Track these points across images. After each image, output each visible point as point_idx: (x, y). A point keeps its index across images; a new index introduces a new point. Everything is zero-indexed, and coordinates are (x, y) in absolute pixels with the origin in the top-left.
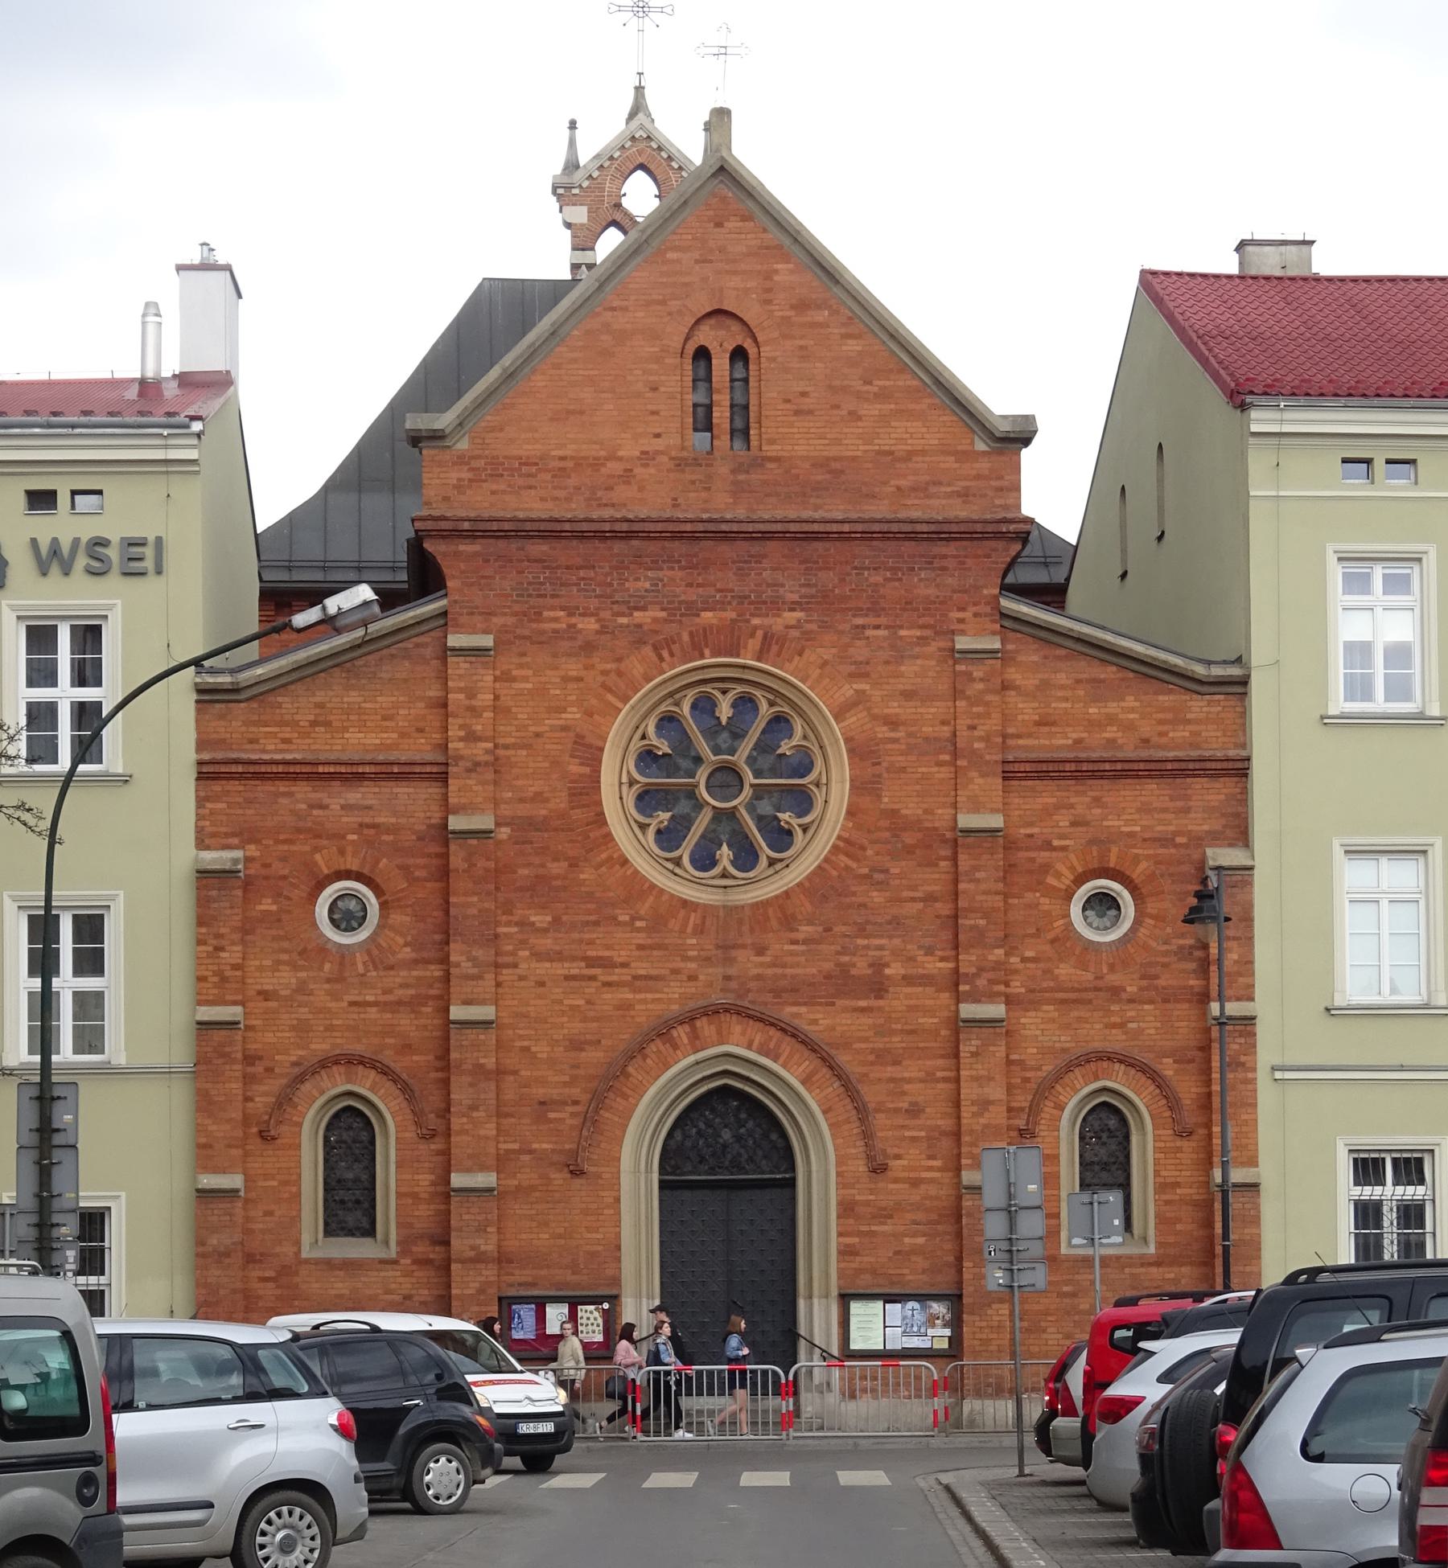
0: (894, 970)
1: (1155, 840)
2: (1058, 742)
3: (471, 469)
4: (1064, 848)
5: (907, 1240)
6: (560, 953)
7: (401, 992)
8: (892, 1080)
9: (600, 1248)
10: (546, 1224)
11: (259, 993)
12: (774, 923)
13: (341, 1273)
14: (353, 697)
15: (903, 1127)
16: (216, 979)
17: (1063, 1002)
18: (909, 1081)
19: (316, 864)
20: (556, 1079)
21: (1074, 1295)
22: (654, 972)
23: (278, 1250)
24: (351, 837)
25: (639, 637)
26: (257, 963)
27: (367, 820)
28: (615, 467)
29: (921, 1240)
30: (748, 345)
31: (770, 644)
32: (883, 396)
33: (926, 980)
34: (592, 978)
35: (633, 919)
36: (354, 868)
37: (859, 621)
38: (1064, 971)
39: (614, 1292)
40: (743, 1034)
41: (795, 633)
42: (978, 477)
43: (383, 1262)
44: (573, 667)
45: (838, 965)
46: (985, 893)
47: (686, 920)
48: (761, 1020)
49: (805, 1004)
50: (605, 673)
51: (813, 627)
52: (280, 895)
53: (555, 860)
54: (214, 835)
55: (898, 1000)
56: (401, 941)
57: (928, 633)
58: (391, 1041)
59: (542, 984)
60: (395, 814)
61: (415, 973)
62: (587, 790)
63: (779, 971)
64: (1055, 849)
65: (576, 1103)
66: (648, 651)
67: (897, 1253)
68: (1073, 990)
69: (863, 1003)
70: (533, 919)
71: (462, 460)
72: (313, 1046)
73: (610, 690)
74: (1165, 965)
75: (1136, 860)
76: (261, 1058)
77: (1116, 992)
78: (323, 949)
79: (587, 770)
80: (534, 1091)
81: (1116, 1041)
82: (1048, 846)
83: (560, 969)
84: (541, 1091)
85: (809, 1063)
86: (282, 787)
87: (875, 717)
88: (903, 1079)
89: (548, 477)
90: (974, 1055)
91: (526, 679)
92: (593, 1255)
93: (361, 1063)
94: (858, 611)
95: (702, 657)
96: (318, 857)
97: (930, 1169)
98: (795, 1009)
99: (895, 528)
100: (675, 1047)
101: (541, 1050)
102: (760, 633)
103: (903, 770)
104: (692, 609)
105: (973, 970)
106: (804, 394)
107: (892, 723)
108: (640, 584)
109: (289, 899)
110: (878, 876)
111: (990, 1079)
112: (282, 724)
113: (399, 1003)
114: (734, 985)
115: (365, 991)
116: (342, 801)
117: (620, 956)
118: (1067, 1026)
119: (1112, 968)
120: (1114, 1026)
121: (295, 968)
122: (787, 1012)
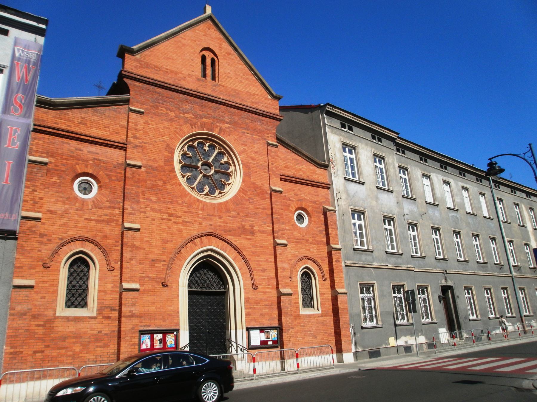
0: (256, 228)
1: (312, 202)
2: (290, 173)
3: (140, 64)
4: (293, 201)
5: (264, 310)
6: (160, 210)
7: (104, 217)
8: (258, 261)
9: (172, 313)
11: (48, 211)
12: (224, 211)
14: (95, 118)
15: (261, 275)
16: (32, 202)
17: (296, 242)
18: (262, 261)
19: (76, 169)
20: (158, 252)
21: (304, 326)
22: (189, 220)
24: (90, 162)
25: (186, 121)
27: (96, 157)
28: (180, 75)
29: (267, 310)
30: (215, 58)
32: (247, 79)
34: (170, 220)
35: (183, 203)
36: (91, 172)
38: (295, 233)
39: (177, 328)
40: (216, 243)
41: (228, 130)
42: (270, 104)
43: (91, 318)
44: (167, 124)
45: (241, 225)
47: (198, 206)
48: (221, 239)
49: (233, 236)
50: (176, 128)
51: (233, 129)
52: (61, 176)
53: (159, 180)
55: (258, 237)
56: (106, 199)
57: (260, 138)
58: (100, 234)
59: (154, 220)
60: (106, 157)
61: (110, 211)
62: (169, 161)
65: (164, 261)
66: (189, 125)
67: (261, 314)
69: (248, 237)
70: (151, 198)
71: (137, 60)
72: (68, 233)
73: (177, 133)
74: (317, 235)
75: (309, 206)
77: (307, 240)
78: (76, 198)
79: (170, 155)
80: (150, 256)
82: (289, 199)
83: (160, 216)
84: (153, 256)
85: (235, 253)
86: (66, 140)
87: (248, 157)
89: (162, 72)
90: (280, 254)
91: (153, 125)
93: (88, 241)
94: (243, 128)
96: (77, 166)
97: (269, 288)
98: (230, 237)
99: (253, 110)
100: (196, 245)
101: (153, 242)
102: (219, 128)
103: (256, 172)
104: (201, 117)
106: (229, 73)
107: (253, 159)
108: (187, 107)
109: (64, 179)
110: (252, 201)
112: (68, 120)
113: (103, 221)
114: (212, 227)
115: (91, 215)
116: (88, 150)
117: (179, 214)
119: (306, 233)
121: (64, 203)
122: (228, 237)
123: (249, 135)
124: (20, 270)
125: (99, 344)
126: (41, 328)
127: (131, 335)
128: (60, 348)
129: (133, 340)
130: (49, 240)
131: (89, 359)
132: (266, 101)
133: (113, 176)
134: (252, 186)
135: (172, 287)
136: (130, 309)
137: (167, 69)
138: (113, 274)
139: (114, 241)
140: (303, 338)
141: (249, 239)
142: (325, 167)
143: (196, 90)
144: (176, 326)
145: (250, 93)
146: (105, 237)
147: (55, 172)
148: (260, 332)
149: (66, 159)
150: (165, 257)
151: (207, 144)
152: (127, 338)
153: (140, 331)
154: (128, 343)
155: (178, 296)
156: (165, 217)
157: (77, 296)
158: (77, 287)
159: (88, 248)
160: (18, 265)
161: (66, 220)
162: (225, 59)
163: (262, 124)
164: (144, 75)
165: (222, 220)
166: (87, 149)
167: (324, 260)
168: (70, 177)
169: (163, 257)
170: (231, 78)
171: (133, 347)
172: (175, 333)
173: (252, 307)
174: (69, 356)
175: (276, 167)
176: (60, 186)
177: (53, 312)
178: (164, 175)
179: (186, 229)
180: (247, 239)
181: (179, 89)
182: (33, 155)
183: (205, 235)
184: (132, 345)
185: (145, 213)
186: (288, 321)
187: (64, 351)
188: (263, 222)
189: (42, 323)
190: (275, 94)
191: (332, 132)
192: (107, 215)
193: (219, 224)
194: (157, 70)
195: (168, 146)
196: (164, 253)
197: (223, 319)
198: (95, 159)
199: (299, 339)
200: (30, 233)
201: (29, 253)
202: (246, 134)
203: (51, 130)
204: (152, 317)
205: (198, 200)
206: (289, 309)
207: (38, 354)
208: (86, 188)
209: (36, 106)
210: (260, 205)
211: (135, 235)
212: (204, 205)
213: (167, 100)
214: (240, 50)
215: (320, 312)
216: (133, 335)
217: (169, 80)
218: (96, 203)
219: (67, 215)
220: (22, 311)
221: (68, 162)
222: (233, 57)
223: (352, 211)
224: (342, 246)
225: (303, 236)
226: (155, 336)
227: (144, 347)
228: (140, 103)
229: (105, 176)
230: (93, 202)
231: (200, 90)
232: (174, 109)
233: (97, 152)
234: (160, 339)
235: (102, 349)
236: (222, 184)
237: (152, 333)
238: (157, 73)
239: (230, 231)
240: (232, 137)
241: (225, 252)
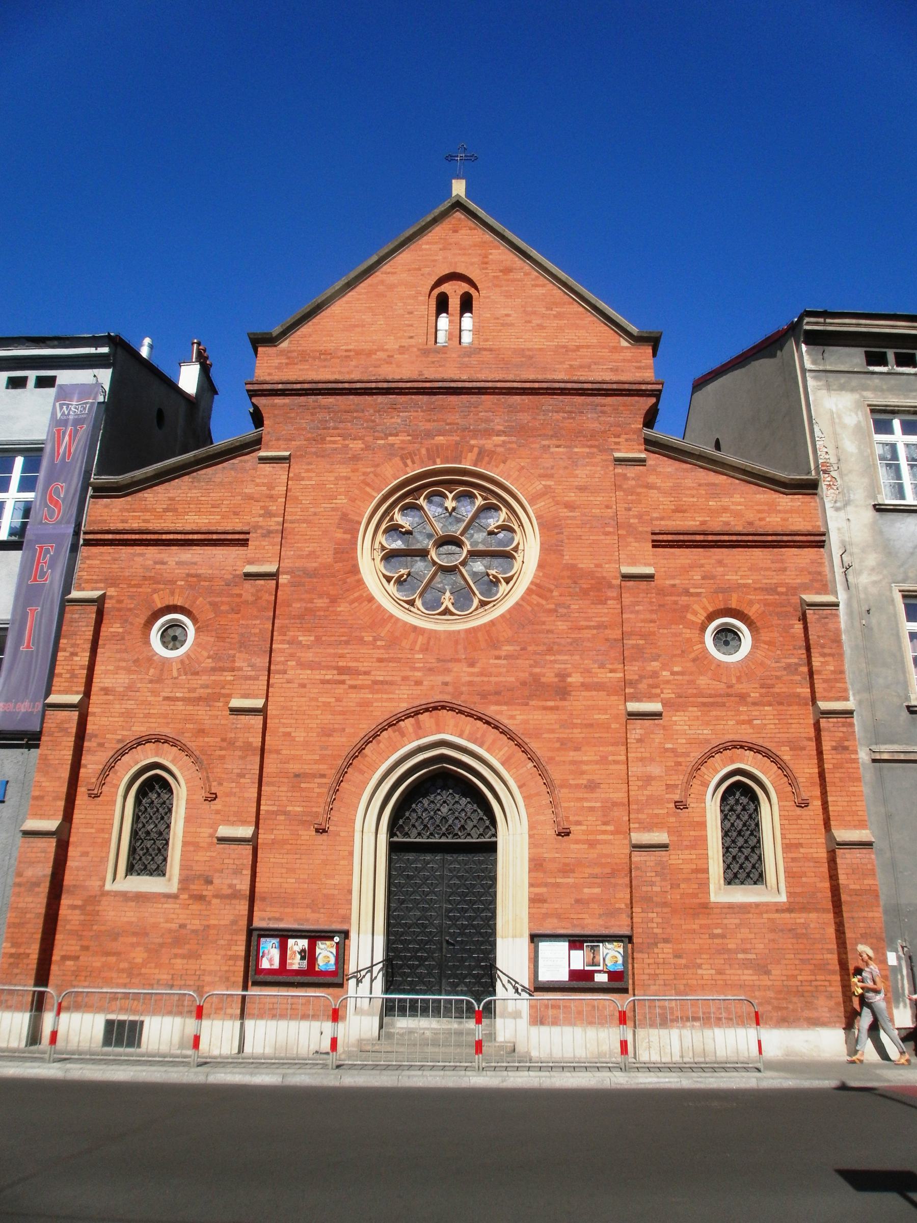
0: (575, 679)
1: (762, 589)
3: (288, 358)
4: (698, 594)
5: (586, 890)
6: (319, 663)
7: (202, 690)
8: (573, 763)
9: (336, 892)
10: (291, 870)
12: (483, 645)
13: (133, 904)
14: (195, 493)
15: (582, 799)
16: (68, 676)
17: (704, 704)
20: (310, 757)
21: (723, 936)
22: (388, 678)
24: (179, 583)
26: (103, 668)
27: (192, 572)
28: (381, 355)
29: (597, 890)
30: (472, 291)
31: (482, 455)
32: (558, 316)
33: (599, 687)
34: (343, 682)
35: (375, 639)
37: (544, 443)
38: (703, 681)
39: (345, 927)
40: (456, 726)
41: (500, 450)
42: (624, 360)
43: (168, 896)
44: (344, 471)
45: (531, 674)
46: (643, 621)
47: (415, 642)
48: (471, 716)
49: (506, 704)
50: (365, 474)
51: (514, 446)
52: (126, 621)
53: (321, 596)
54: (87, 581)
55: (579, 702)
56: (205, 654)
57: (595, 450)
58: (191, 726)
59: (303, 686)
60: (211, 567)
61: (213, 678)
63: (486, 679)
64: (692, 595)
65: (323, 776)
67: (578, 901)
68: (710, 696)
70: (300, 638)
71: (282, 353)
72: (134, 729)
73: (368, 485)
74: (777, 678)
75: (751, 603)
76: (96, 736)
77: (743, 698)
78: (151, 659)
79: (348, 536)
80: (292, 766)
81: (745, 734)
82: (687, 593)
83: (318, 675)
84: (297, 766)
85: (508, 747)
86: (138, 549)
88: (582, 762)
89: (338, 361)
90: (639, 741)
91: (310, 479)
92: (327, 896)
93: (166, 742)
94: (545, 436)
95: (435, 463)
96: (155, 596)
97: (604, 832)
99: (569, 386)
100: (403, 735)
101: (300, 735)
102: (476, 450)
103: (579, 537)
104: (429, 434)
105: (636, 677)
106: (507, 315)
107: (570, 506)
108: (393, 420)
109: (131, 624)
110: (562, 611)
111: (652, 760)
112: (145, 510)
113: (200, 699)
114: (450, 689)
115: (175, 690)
116: (177, 559)
117: (363, 666)
118: (707, 724)
119: (739, 679)
120: (743, 722)
121: (129, 671)
122: (492, 710)
123: (561, 450)
124: (41, 803)
125: (180, 951)
126: (77, 912)
127: (229, 937)
128: (108, 954)
130: (101, 745)
131: (159, 981)
132: (616, 356)
133: (222, 603)
134: (566, 573)
135: (337, 834)
136: (229, 881)
137: (349, 351)
138: (213, 807)
139: (218, 740)
140: (720, 972)
141: (551, 709)
142: (810, 487)
143: (415, 377)
144: (342, 922)
145: (564, 347)
146: (201, 732)
147: (117, 613)
148: (570, 948)
149: (135, 586)
150: (325, 767)
151: (450, 496)
152: (222, 942)
154: (222, 952)
155: (351, 854)
156: (328, 677)
157: (147, 854)
158: (153, 835)
159: (167, 757)
160: (37, 793)
161: (130, 705)
162: (496, 286)
163: (592, 415)
164: (293, 378)
165: (476, 670)
166: (176, 559)
167: (803, 748)
168: (141, 620)
169: (321, 767)
170: (512, 325)
171: (231, 963)
172: (337, 939)
173: (549, 880)
174: (123, 971)
175: (640, 516)
176: (123, 639)
177: (99, 883)
178: (333, 584)
179: (381, 700)
180: (545, 708)
181: (373, 385)
182: (83, 589)
183: (427, 710)
184: (232, 958)
185: (285, 672)
186: (652, 921)
187: (113, 959)
188: (595, 662)
189: (79, 903)
190: (634, 330)
191: (829, 388)
192: (207, 687)
193: (468, 679)
194: (325, 360)
195: (344, 517)
197: (489, 910)
198: (188, 575)
199: (706, 972)
200: (59, 734)
202: (553, 450)
203: (110, 537)
205: (415, 628)
206: (656, 889)
207: (69, 963)
208: (172, 637)
209: (92, 497)
210: (588, 619)
211: (252, 722)
213: (348, 416)
214: (534, 253)
215: (783, 898)
216: (235, 937)
217: (352, 372)
218: (187, 666)
219: (134, 693)
220: (34, 880)
221: (140, 590)
222: (520, 275)
223: (904, 597)
224: (860, 703)
225: (730, 687)
226: (291, 942)
227: (265, 964)
228: (286, 440)
229: (208, 606)
230: (182, 662)
231: (430, 374)
233: (195, 560)
234: (303, 951)
235: (185, 961)
236: (491, 581)
237: (283, 936)
238: (325, 367)
239: (497, 693)
240: (511, 464)
241: (481, 746)
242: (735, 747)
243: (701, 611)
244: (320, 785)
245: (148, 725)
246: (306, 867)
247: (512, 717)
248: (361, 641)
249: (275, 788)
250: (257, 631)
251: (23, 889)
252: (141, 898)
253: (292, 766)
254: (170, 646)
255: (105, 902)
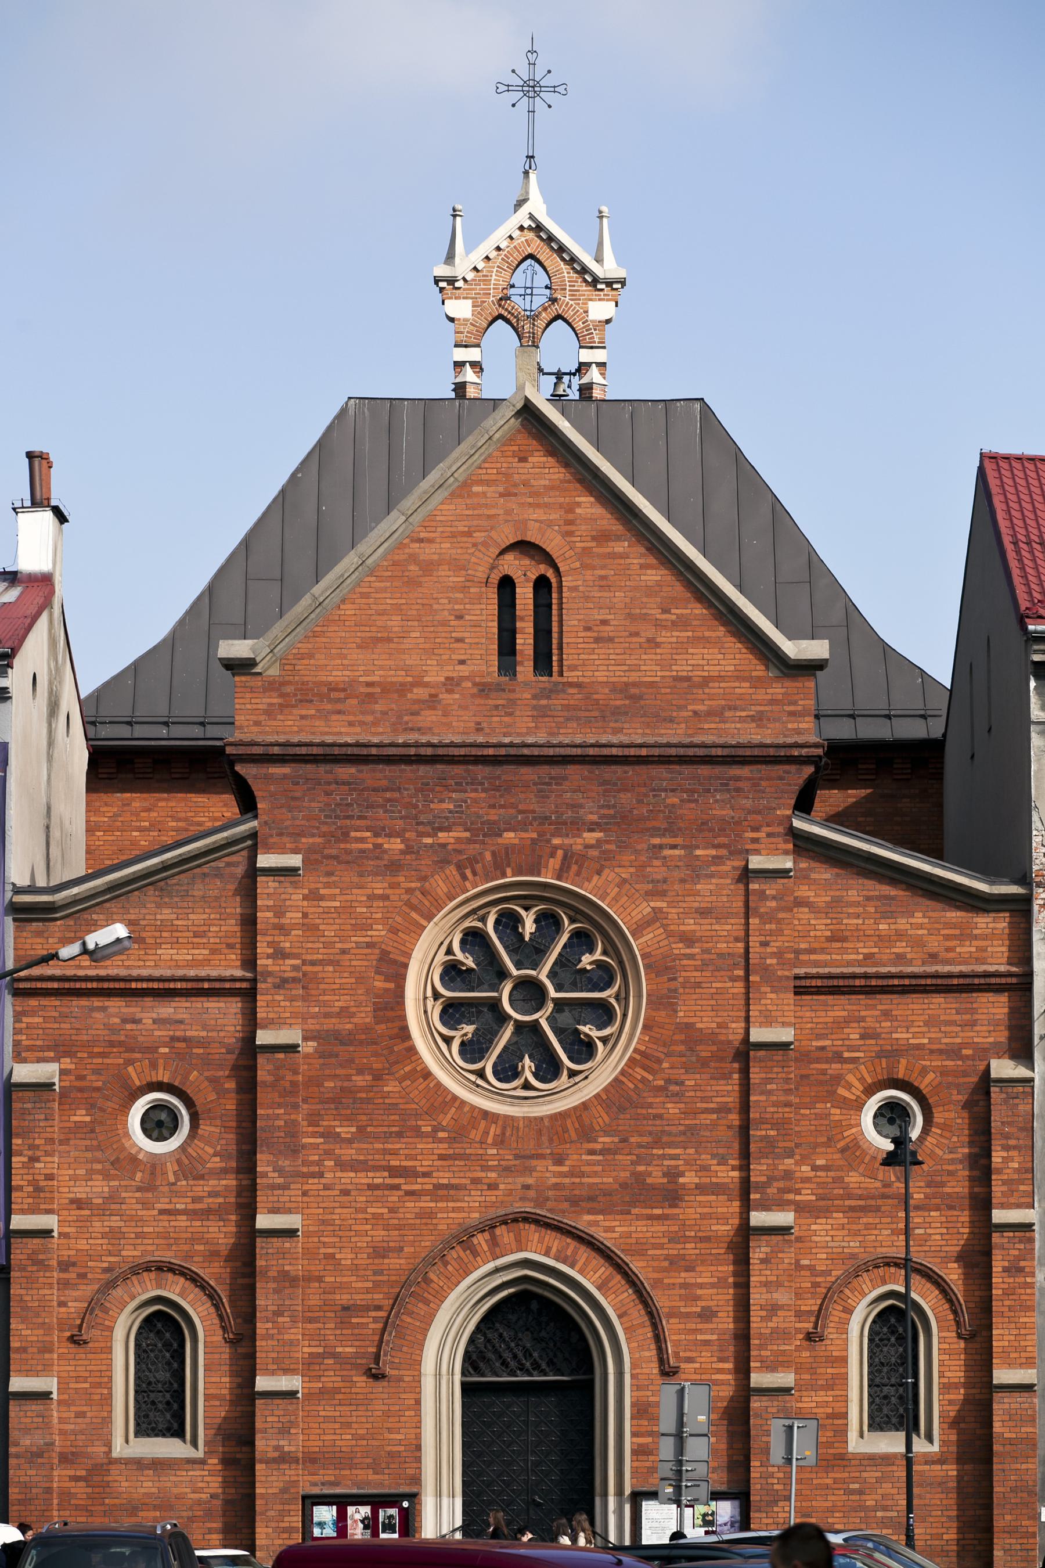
1: (941, 1052)
2: (846, 960)
7: (211, 1200)
8: (684, 1286)
10: (348, 1425)
11: (73, 1201)
14: (166, 914)
16: (31, 1189)
17: (852, 1209)
19: (129, 1077)
20: (360, 1285)
22: (454, 1181)
23: (89, 1449)
24: (163, 1050)
25: (443, 857)
27: (178, 1034)
28: (420, 693)
30: (550, 574)
31: (570, 862)
32: (681, 623)
33: (717, 1189)
34: (397, 1187)
35: (436, 1130)
37: (657, 841)
38: (853, 1178)
39: (414, 1490)
40: (541, 1241)
41: (594, 853)
42: (773, 702)
44: (379, 887)
45: (634, 1174)
49: (601, 1212)
50: (409, 891)
51: (613, 847)
52: (93, 1106)
53: (360, 1072)
55: (691, 1210)
56: (211, 1151)
57: (724, 852)
60: (205, 1027)
61: (224, 1182)
63: (577, 1180)
65: (378, 1308)
66: (451, 870)
68: (860, 1198)
70: (338, 1130)
72: (124, 1253)
73: (413, 908)
74: (950, 1173)
75: (924, 1071)
76: (74, 1264)
79: (392, 986)
80: (338, 1297)
82: (838, 1058)
83: (363, 1179)
85: (604, 1270)
86: (97, 1002)
90: (763, 1261)
91: (332, 897)
94: (655, 832)
95: (504, 876)
96: (130, 1069)
100: (475, 1253)
101: (346, 1257)
102: (560, 853)
103: (698, 985)
104: (495, 830)
105: (764, 1179)
106: (604, 622)
107: (688, 940)
111: (779, 1284)
114: (532, 1194)
115: (174, 1200)
116: (155, 1016)
117: (423, 1164)
121: (107, 1177)
122: (584, 1222)
123: (677, 852)
127: (281, 1507)
129: (286, 1519)
130: (82, 1276)
135: (400, 1379)
136: (275, 1443)
144: (410, 1484)
147: (79, 1095)
149: (103, 1055)
150: (381, 1296)
152: (271, 1513)
153: (304, 1498)
156: (379, 1181)
161: (115, 1222)
165: (565, 1169)
169: (376, 1296)
171: (286, 1536)
178: (376, 1054)
183: (505, 1223)
184: (285, 1530)
185: (321, 1175)
188: (714, 1156)
194: (338, 700)
196: (377, 1284)
198: (173, 1039)
201: (38, 1315)
203: (55, 985)
204: (343, 1460)
205: (485, 1114)
212: (504, 1128)
215: (936, 1448)
219: (117, 1206)
226: (351, 1510)
228: (290, 835)
229: (206, 1083)
232: (399, 824)
234: (366, 1518)
237: (342, 1502)
238: (339, 712)
239: (591, 1199)
241: (572, 1267)
242: (888, 1264)
243: (856, 1083)
244: (375, 1320)
245: (142, 1248)
246: (364, 1420)
247: (610, 1229)
248: (417, 1132)
249: (320, 1325)
250: (282, 1123)
251: (23, 1460)
252: (159, 1465)
253: (338, 1297)
254: (155, 1134)
255: (114, 1471)
